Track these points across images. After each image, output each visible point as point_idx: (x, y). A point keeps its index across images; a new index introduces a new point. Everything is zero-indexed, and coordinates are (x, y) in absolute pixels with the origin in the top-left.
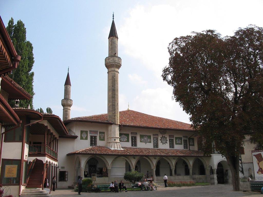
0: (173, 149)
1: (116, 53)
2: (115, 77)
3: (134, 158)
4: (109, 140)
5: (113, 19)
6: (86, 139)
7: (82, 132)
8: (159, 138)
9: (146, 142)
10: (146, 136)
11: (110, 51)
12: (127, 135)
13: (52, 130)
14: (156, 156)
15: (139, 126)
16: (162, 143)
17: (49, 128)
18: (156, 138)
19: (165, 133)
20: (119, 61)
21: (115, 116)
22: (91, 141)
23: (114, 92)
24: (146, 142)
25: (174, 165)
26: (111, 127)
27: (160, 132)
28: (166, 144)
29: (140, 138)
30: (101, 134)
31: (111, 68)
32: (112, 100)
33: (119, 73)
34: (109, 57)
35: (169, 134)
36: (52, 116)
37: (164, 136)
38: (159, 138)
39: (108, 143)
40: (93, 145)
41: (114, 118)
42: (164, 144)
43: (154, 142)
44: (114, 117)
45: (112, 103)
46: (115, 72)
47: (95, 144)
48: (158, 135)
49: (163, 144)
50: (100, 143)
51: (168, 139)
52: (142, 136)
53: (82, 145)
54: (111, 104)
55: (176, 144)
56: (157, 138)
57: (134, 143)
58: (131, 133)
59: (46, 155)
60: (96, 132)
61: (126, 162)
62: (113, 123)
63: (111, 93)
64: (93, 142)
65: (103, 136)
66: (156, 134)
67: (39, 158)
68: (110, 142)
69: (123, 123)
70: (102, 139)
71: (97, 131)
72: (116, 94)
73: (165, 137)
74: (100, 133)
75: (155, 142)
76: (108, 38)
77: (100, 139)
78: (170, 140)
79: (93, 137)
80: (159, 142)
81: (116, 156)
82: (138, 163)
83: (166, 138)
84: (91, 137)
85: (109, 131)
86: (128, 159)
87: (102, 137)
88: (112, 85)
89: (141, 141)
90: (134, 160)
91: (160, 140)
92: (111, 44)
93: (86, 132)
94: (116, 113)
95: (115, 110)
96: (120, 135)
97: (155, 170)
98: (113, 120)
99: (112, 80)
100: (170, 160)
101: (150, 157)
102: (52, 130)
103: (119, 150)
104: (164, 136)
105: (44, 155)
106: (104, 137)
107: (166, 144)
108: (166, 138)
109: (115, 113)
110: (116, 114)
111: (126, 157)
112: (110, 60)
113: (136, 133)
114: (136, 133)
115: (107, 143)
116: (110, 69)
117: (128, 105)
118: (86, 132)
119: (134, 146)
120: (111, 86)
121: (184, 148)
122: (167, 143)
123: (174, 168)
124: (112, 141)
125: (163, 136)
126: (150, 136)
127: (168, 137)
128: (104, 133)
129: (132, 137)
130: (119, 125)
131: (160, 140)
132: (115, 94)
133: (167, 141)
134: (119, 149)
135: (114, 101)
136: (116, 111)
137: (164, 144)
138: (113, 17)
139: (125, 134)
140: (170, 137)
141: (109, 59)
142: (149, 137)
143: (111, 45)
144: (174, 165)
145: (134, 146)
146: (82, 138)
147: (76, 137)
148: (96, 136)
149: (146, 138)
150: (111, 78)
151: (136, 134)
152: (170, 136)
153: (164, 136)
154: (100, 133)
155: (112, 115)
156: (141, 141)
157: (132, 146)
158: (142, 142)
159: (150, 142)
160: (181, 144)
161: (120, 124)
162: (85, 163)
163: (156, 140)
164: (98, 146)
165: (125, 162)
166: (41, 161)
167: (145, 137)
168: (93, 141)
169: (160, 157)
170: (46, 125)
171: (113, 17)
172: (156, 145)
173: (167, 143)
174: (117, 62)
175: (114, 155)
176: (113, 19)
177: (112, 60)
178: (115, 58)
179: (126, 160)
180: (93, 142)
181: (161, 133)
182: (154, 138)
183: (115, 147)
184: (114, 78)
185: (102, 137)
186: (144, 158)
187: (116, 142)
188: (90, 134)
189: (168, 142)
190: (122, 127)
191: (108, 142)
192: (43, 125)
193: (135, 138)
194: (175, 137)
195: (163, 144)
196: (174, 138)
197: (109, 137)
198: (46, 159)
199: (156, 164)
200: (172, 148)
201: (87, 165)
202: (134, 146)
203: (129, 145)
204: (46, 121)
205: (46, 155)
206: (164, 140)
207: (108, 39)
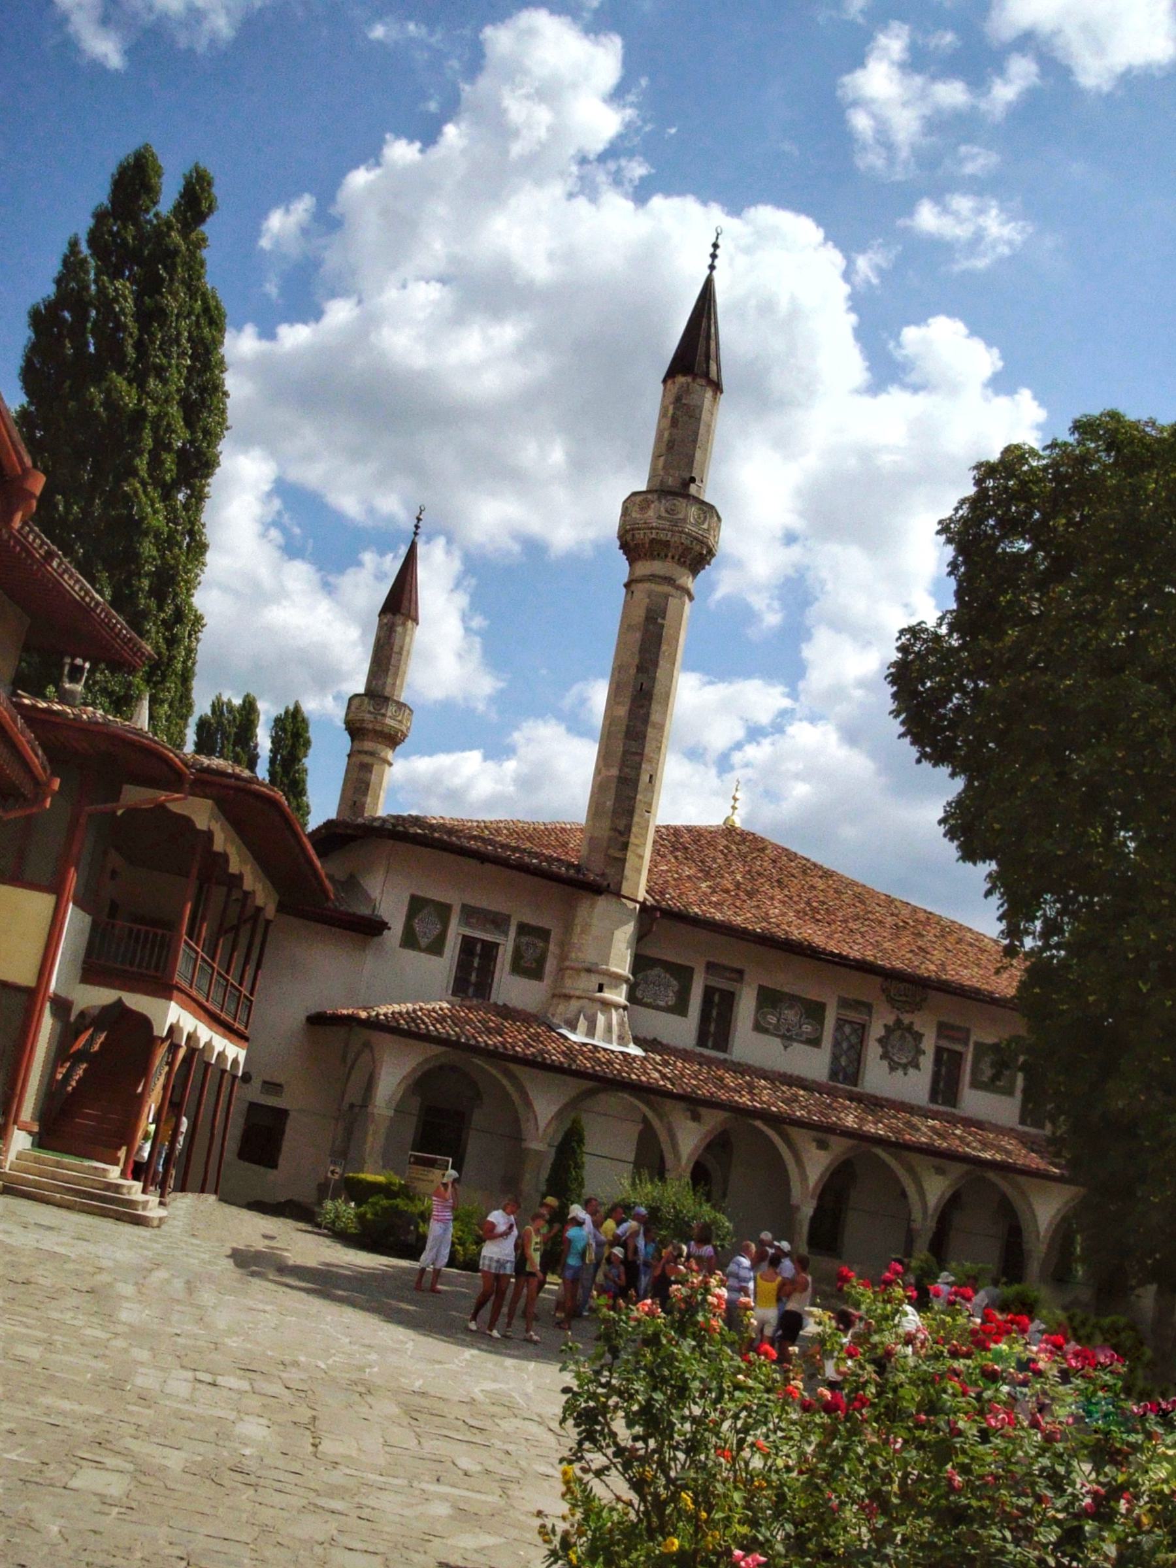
0: (953, 1110)
1: (693, 480)
2: (664, 618)
3: (696, 1117)
4: (568, 982)
6: (436, 948)
7: (417, 905)
8: (877, 1030)
9: (790, 1039)
10: (794, 1000)
11: (662, 458)
12: (684, 974)
13: (239, 863)
14: (832, 1129)
15: (745, 933)
16: (885, 1063)
17: (219, 844)
18: (857, 1026)
19: (916, 1006)
20: (705, 526)
21: (625, 846)
22: (463, 967)
23: (642, 706)
24: (788, 1039)
25: (930, 1212)
26: (592, 906)
28: (911, 1071)
30: (524, 940)
31: (654, 559)
32: (625, 752)
33: (691, 598)
34: (649, 496)
35: (945, 1019)
36: (241, 784)
37: (906, 1022)
38: (877, 1030)
39: (555, 1001)
40: (471, 991)
41: (616, 859)
42: (900, 1072)
43: (837, 1044)
44: (618, 855)
45: (620, 771)
46: (667, 589)
47: (483, 988)
48: (868, 1008)
49: (892, 1069)
50: (510, 988)
51: (929, 1045)
52: (769, 999)
53: (410, 985)
54: (614, 772)
55: (976, 1084)
56: (863, 1026)
57: (716, 1027)
59: (175, 993)
60: (499, 922)
61: (641, 1127)
62: (605, 883)
63: (622, 711)
64: (473, 978)
65: (538, 951)
67: (137, 1002)
68: (568, 997)
69: (672, 900)
70: (529, 967)
71: (507, 919)
72: (655, 717)
73: (916, 1028)
74: (523, 929)
75: (845, 1045)
76: (665, 381)
77: (518, 968)
78: (939, 1051)
79: (475, 946)
80: (873, 1051)
81: (590, 1084)
82: (719, 1146)
84: (468, 945)
85: (578, 929)
86: (660, 1117)
87: (529, 955)
88: (636, 661)
89: (759, 1027)
90: (691, 1124)
92: (673, 417)
93: (443, 911)
94: (634, 829)
95: (630, 813)
96: (640, 963)
97: (808, 1210)
98: (607, 871)
99: (646, 631)
100: (911, 1170)
101: (793, 1131)
102: (239, 863)
103: (613, 1052)
104: (906, 1022)
105: (164, 989)
106: (541, 961)
108: (918, 1037)
109: (628, 828)
110: (633, 840)
111: (648, 1103)
112: (651, 513)
113: (741, 972)
114: (741, 972)
115: (554, 996)
116: (646, 567)
117: (735, 799)
118: (443, 911)
119: (710, 1044)
120: (633, 671)
121: (1023, 1121)
122: (917, 1067)
123: (931, 1224)
124: (578, 993)
125: (898, 1022)
126: (822, 1007)
127: (934, 1029)
128: (544, 934)
129: (709, 992)
130: (643, 904)
132: (646, 719)
133: (922, 1059)
134: (615, 1047)
135: (637, 758)
136: (636, 819)
137: (900, 1072)
139: (669, 967)
140: (947, 1037)
141: (644, 508)
143: (674, 422)
144: (930, 1212)
145: (713, 1048)
146: (409, 940)
147: (373, 928)
148: (498, 944)
149: (791, 1015)
150: (639, 614)
151: (734, 975)
152: (944, 1029)
153: (906, 1019)
154: (523, 929)
155: (610, 839)
156: (759, 1027)
157: (702, 1040)
158: (765, 1031)
159: (815, 1042)
160: (1003, 1093)
161: (650, 901)
162: (403, 1086)
163: (854, 1039)
164: (495, 1004)
165: (632, 1131)
166: (144, 1023)
167: (791, 1007)
168: (474, 974)
169: (856, 1142)
170: (201, 823)
173: (917, 1067)
174: (688, 528)
175: (580, 1074)
177: (664, 514)
178: (681, 503)
179: (645, 1120)
180: (473, 978)
181: (891, 1001)
182: (840, 1023)
183: (591, 1032)
184: (660, 621)
185: (529, 955)
186: (756, 1128)
187: (607, 1005)
188: (459, 924)
189: (927, 1062)
190: (655, 919)
191: (557, 992)
192: (188, 821)
193: (729, 999)
194: (977, 1044)
195: (892, 1069)
196: (966, 1044)
197: (567, 963)
198: (175, 1015)
199: (822, 1176)
200: (944, 1104)
201: (415, 1103)
202: (710, 1044)
203: (682, 1030)
204: (210, 802)
205: (175, 993)
206: (900, 1046)
207: (661, 386)
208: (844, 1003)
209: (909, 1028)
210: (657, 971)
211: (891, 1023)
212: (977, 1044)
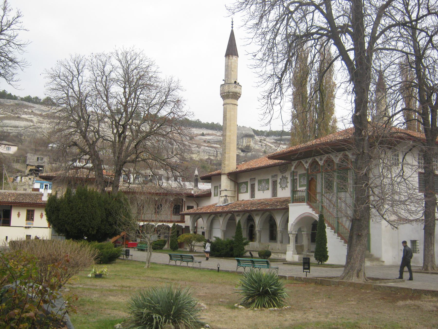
5: (232, 27)
8: (279, 181)
24: (263, 190)
27: (280, 170)
28: (286, 188)
29: (258, 185)
48: (276, 175)
49: (282, 189)
51: (289, 180)
58: (251, 179)
66: (275, 175)
80: (279, 186)
83: (287, 178)
91: (279, 183)
107: (286, 188)
114: (255, 178)
122: (287, 187)
125: (283, 176)
126: (268, 179)
131: (279, 183)
138: (232, 25)
139: (244, 183)
142: (267, 181)
149: (263, 184)
159: (268, 189)
171: (232, 25)
172: (274, 193)
173: (287, 187)
176: (232, 27)
189: (289, 185)
194: (299, 175)
195: (282, 189)
208: (273, 177)
209: (285, 177)
210: (243, 184)
211: (281, 177)
212: (299, 175)
